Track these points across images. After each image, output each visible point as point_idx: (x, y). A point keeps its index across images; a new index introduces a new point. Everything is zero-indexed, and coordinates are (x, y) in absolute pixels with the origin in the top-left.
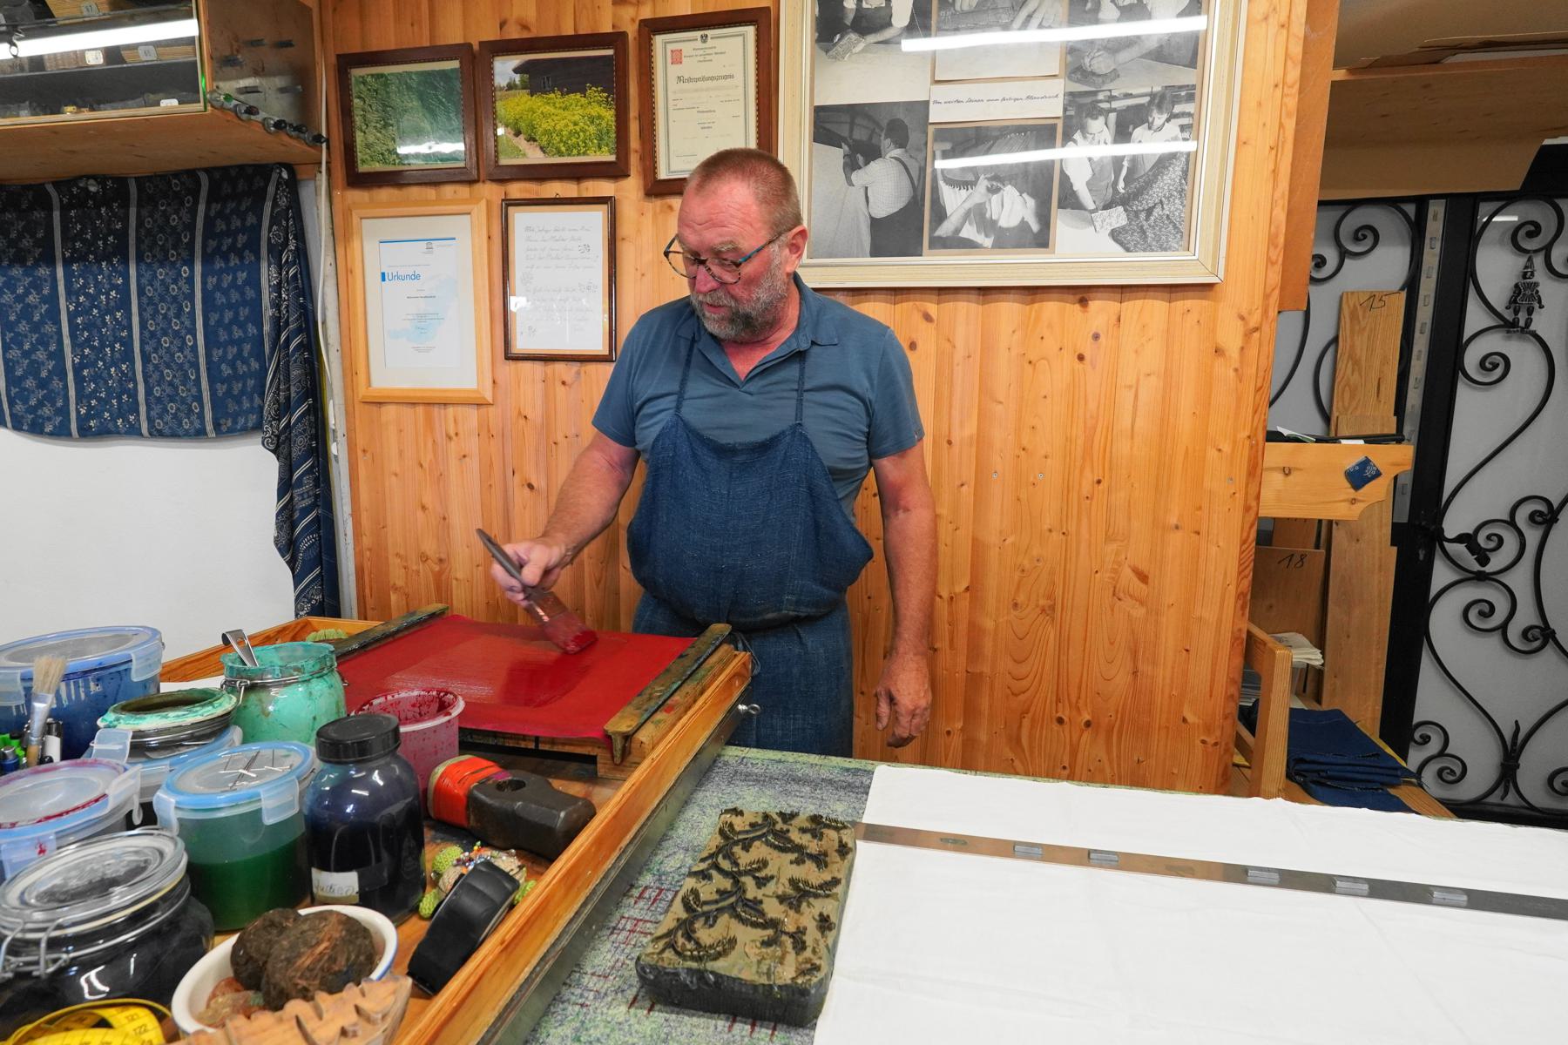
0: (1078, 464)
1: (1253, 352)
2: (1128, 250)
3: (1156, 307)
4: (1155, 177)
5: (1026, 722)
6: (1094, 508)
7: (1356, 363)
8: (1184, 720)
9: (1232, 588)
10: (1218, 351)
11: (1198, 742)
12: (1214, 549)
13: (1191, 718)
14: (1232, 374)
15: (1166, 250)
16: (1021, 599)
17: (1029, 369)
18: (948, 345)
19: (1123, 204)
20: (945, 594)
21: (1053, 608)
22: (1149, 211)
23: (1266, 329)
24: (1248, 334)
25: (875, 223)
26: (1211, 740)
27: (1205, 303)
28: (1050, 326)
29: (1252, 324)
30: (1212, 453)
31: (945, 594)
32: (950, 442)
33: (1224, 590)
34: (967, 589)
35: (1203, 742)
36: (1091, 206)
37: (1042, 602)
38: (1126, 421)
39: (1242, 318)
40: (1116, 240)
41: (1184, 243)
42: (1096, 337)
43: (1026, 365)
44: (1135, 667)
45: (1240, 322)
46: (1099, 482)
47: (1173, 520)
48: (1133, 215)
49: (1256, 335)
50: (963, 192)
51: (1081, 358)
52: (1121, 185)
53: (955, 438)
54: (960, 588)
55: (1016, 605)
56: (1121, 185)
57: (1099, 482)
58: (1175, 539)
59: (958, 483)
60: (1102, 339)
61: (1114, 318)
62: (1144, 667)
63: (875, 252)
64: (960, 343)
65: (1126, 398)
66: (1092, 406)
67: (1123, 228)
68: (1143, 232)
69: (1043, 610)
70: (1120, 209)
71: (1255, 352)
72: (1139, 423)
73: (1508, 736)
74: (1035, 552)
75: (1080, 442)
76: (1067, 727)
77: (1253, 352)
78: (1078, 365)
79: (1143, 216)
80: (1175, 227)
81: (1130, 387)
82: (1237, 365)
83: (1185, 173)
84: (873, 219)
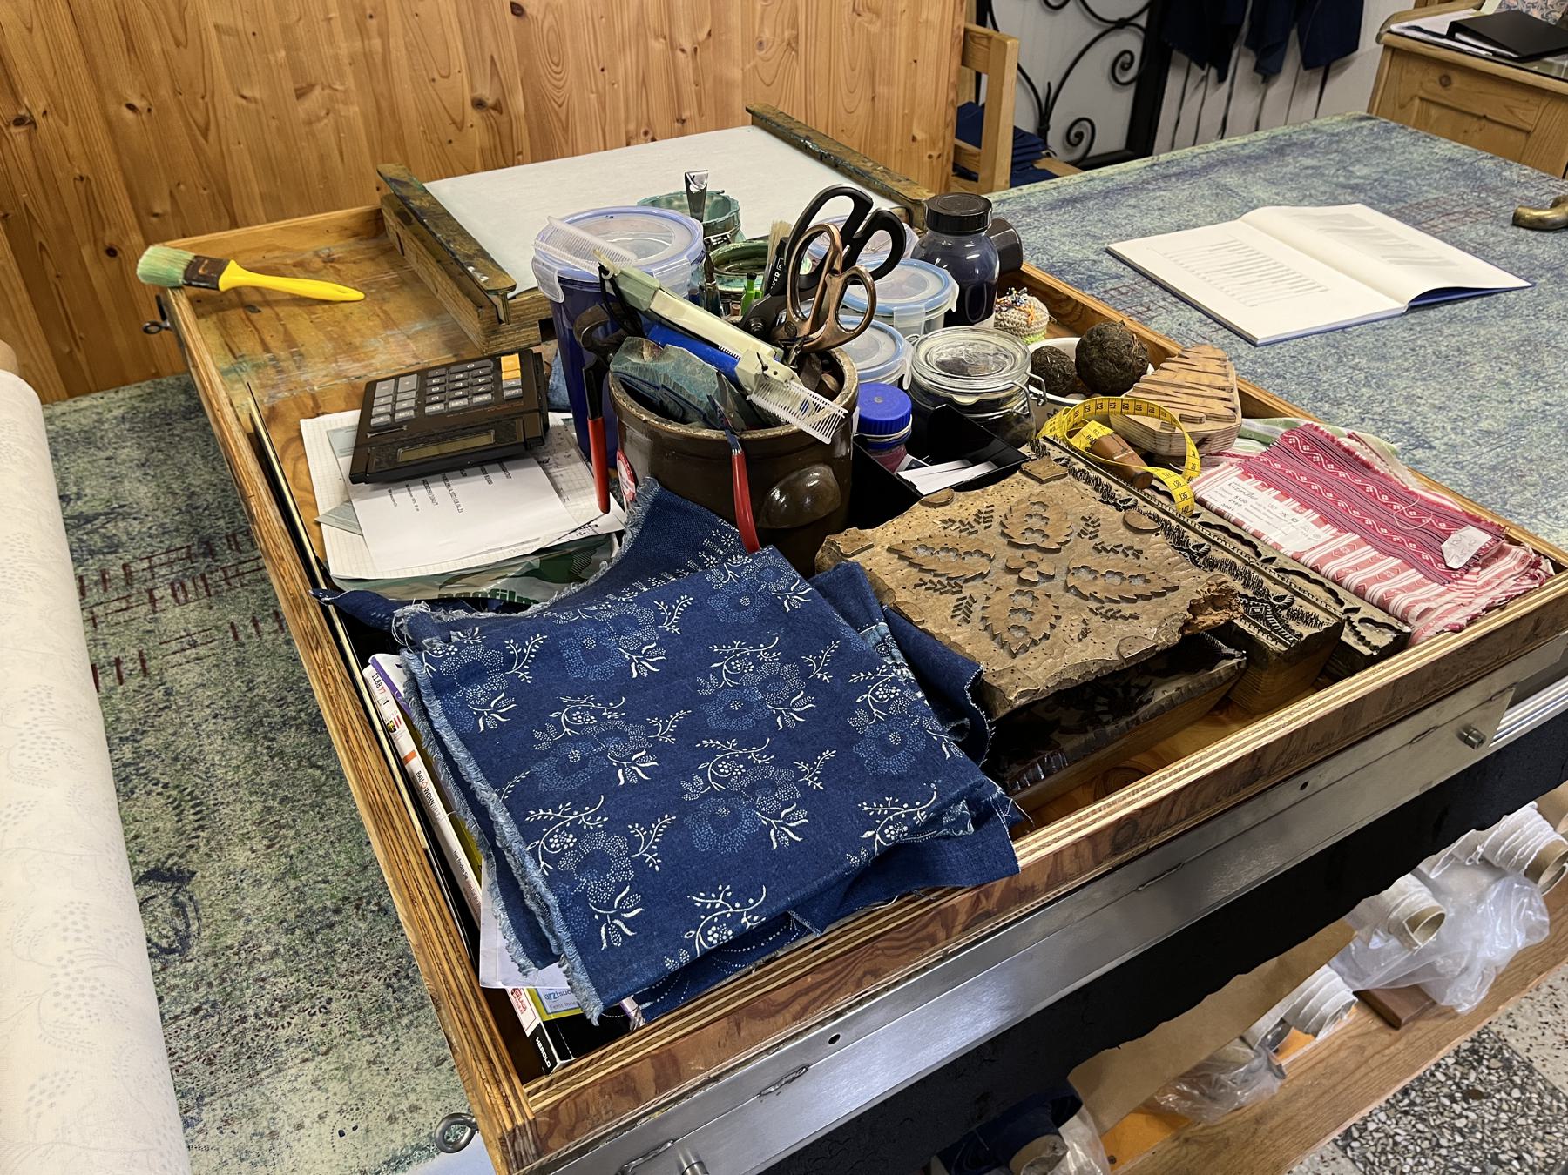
8: (914, 139)
11: (926, 159)
13: (920, 135)
16: (767, 34)
26: (935, 154)
31: (688, 47)
54: (702, 35)
62: (881, 90)
73: (1042, 94)
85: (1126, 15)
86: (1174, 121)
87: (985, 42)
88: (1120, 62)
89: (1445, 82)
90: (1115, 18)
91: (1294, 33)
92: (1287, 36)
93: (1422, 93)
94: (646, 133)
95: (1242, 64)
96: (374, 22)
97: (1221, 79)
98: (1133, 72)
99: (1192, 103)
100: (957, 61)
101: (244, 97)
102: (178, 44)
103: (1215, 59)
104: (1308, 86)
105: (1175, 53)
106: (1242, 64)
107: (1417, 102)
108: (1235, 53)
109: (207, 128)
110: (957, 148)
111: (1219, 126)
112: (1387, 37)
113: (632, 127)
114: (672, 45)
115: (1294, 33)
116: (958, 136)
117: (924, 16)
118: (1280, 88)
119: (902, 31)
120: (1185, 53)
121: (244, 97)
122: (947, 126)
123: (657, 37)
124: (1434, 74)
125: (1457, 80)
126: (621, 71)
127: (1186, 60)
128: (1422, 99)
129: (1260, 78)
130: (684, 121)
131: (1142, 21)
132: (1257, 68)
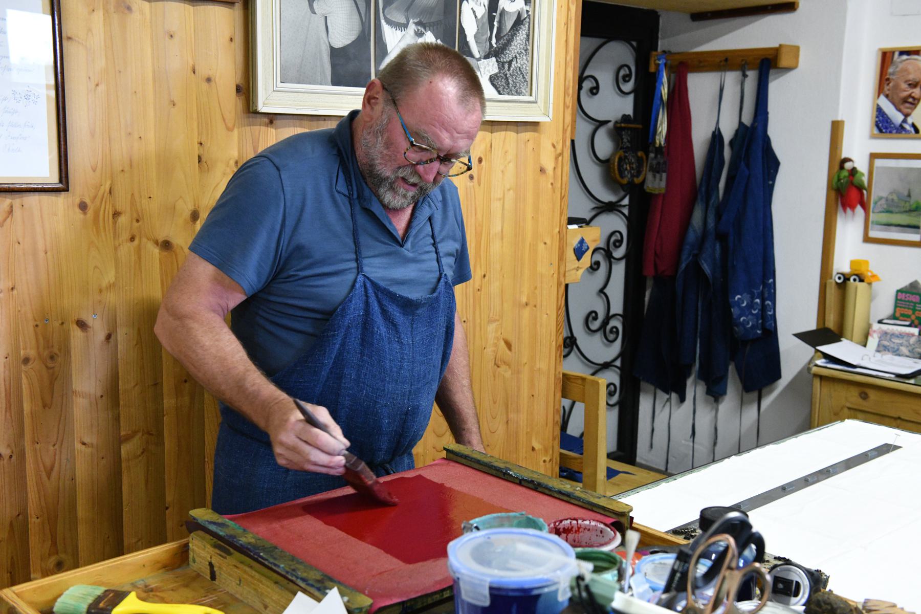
2: (500, 93)
3: (511, 135)
4: (513, 36)
8: (533, 449)
9: (554, 343)
10: (542, 170)
11: (542, 463)
12: (545, 316)
14: (550, 186)
15: (519, 94)
19: (496, 56)
22: (510, 63)
25: (336, 54)
26: (547, 459)
27: (536, 134)
30: (541, 246)
33: (551, 345)
35: (544, 461)
36: (477, 55)
38: (497, 228)
39: (554, 146)
40: (493, 85)
41: (528, 89)
44: (507, 417)
46: (484, 276)
47: (524, 300)
48: (501, 65)
50: (399, 32)
52: (494, 41)
56: (494, 41)
57: (484, 276)
58: (526, 312)
62: (512, 416)
63: (336, 82)
66: (479, 216)
67: (496, 75)
68: (507, 79)
70: (494, 59)
79: (506, 66)
80: (524, 77)
81: (500, 199)
83: (528, 36)
84: (332, 48)
85: (609, 359)
86: (649, 430)
87: (580, 382)
89: (864, 396)
90: (601, 361)
91: (731, 368)
92: (727, 370)
93: (848, 405)
95: (694, 389)
96: (187, 385)
97: (682, 399)
100: (559, 394)
101: (84, 444)
102: (44, 406)
103: (675, 387)
104: (750, 402)
105: (644, 385)
106: (694, 389)
107: (846, 410)
108: (690, 382)
109: (52, 469)
110: (561, 454)
111: (690, 432)
112: (815, 369)
115: (731, 368)
116: (562, 447)
117: (537, 366)
118: (728, 404)
119: (525, 377)
120: (652, 383)
121: (84, 444)
122: (554, 439)
124: (854, 393)
125: (873, 395)
127: (652, 388)
128: (849, 408)
129: (712, 399)
131: (618, 363)
132: (709, 392)
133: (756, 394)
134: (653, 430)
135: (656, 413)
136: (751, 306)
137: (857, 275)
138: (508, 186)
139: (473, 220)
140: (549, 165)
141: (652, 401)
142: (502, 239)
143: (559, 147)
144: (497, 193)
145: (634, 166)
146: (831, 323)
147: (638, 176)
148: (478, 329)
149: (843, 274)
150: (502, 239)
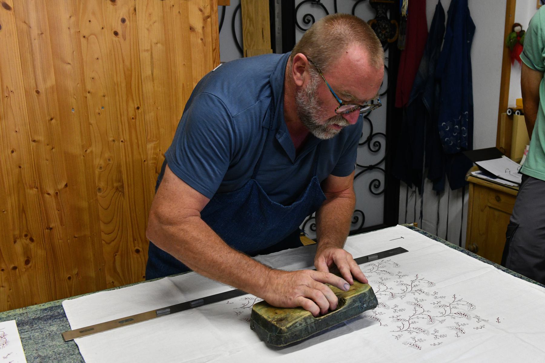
0: (124, 98)
1: (208, 29)
5: (118, 258)
6: (138, 123)
7: (251, 20)
10: (192, 29)
14: (200, 41)
16: (102, 185)
17: (83, 40)
18: (25, 26)
20: (52, 192)
21: (122, 187)
23: (213, 17)
24: (205, 19)
28: (94, 13)
29: (206, 14)
31: (52, 192)
32: (38, 92)
34: (66, 185)
37: (115, 185)
38: (147, 71)
42: (123, 21)
43: (82, 39)
45: (200, 13)
46: (138, 108)
49: (209, 20)
51: (116, 34)
53: (42, 88)
55: (99, 189)
57: (138, 108)
59: (48, 118)
60: (127, 22)
61: (132, 9)
64: (33, 22)
65: (145, 56)
69: (117, 189)
71: (210, 29)
72: (156, 72)
74: (107, 155)
75: (124, 85)
76: (141, 253)
77: (208, 29)
78: (115, 38)
81: (147, 50)
82: (202, 37)
86: (405, 211)
88: (374, 184)
94: (26, 236)
95: (428, 188)
98: (382, 188)
99: (411, 202)
106: (428, 188)
113: (17, 232)
114: (42, 191)
118: (444, 199)
123: (31, 188)
126: (9, 206)
130: (51, 229)
132: (434, 188)
133: (461, 194)
134: (406, 212)
135: (409, 200)
136: (452, 130)
137: (519, 110)
138: (154, 41)
139: (121, 66)
140: (198, 24)
141: (406, 192)
142: (153, 81)
143: (207, 12)
144: (145, 45)
145: (388, 30)
146: (503, 145)
147: (391, 36)
148: (135, 147)
149: (511, 109)
150: (153, 81)
